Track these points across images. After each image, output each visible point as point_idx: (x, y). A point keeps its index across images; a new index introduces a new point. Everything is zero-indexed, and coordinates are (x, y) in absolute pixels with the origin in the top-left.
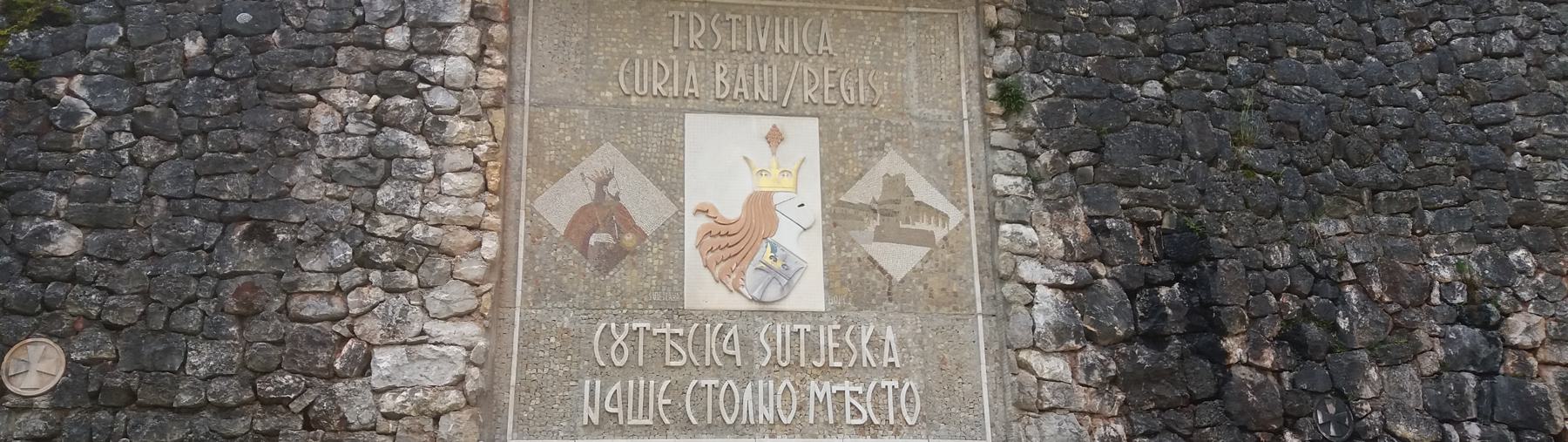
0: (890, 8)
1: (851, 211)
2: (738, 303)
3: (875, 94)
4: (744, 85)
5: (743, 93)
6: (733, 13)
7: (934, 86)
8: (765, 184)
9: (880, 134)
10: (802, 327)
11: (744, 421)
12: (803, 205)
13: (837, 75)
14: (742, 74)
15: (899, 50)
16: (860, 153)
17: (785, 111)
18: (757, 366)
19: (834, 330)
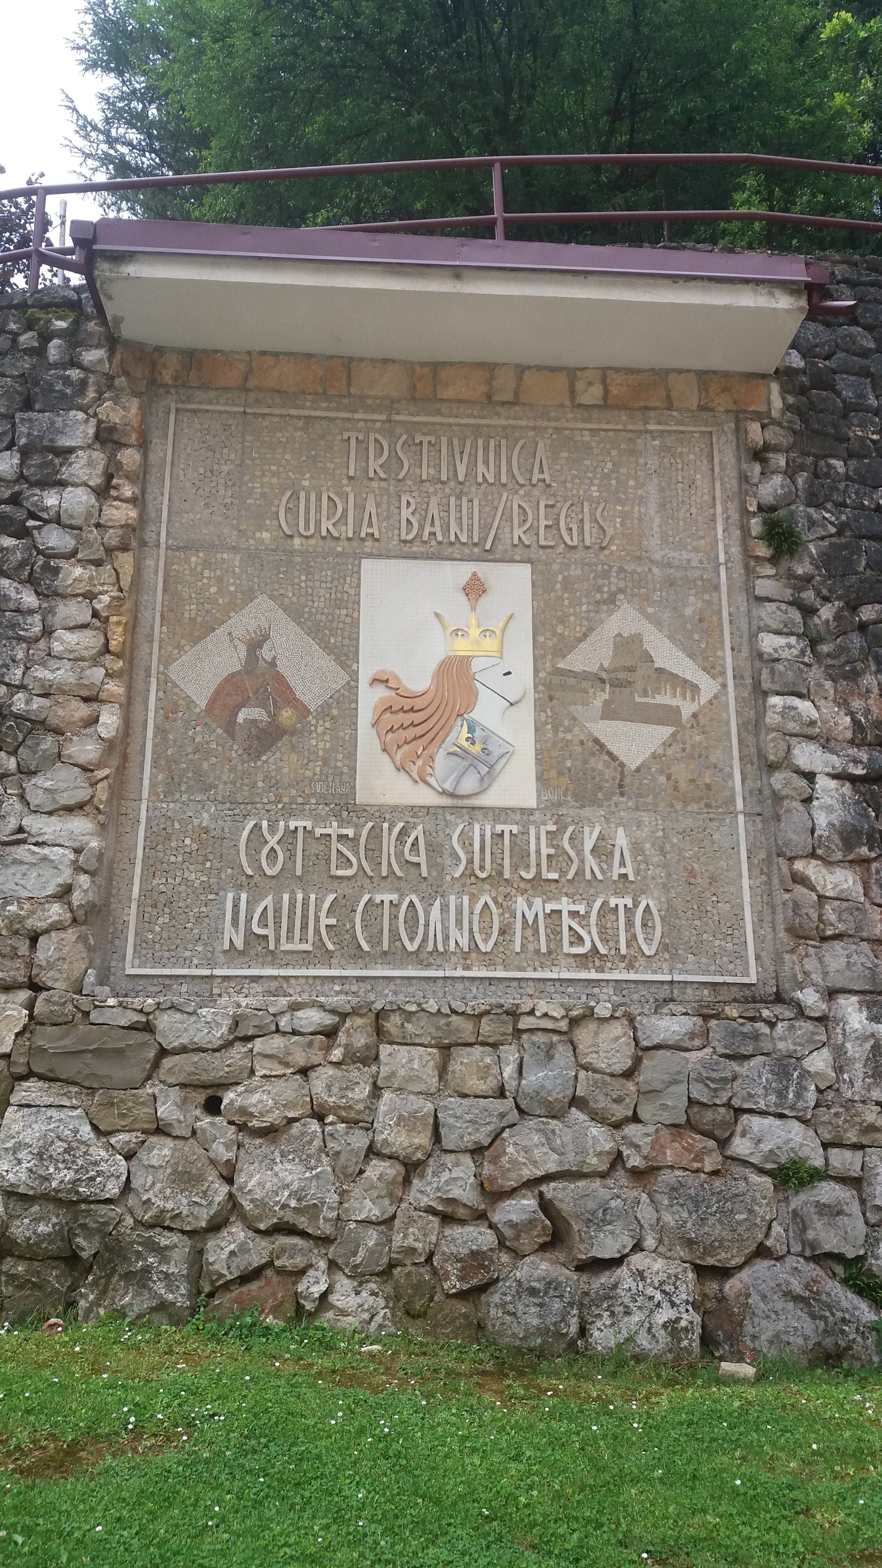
0: (625, 426)
1: (572, 681)
2: (424, 797)
3: (604, 531)
4: (437, 522)
5: (435, 534)
6: (424, 434)
7: (681, 523)
8: (461, 647)
9: (610, 583)
10: (507, 828)
11: (430, 947)
12: (509, 673)
13: (556, 510)
14: (434, 510)
15: (636, 478)
16: (584, 608)
17: (489, 555)
18: (448, 878)
19: (547, 832)
